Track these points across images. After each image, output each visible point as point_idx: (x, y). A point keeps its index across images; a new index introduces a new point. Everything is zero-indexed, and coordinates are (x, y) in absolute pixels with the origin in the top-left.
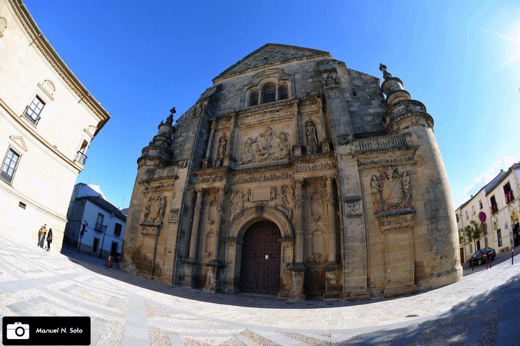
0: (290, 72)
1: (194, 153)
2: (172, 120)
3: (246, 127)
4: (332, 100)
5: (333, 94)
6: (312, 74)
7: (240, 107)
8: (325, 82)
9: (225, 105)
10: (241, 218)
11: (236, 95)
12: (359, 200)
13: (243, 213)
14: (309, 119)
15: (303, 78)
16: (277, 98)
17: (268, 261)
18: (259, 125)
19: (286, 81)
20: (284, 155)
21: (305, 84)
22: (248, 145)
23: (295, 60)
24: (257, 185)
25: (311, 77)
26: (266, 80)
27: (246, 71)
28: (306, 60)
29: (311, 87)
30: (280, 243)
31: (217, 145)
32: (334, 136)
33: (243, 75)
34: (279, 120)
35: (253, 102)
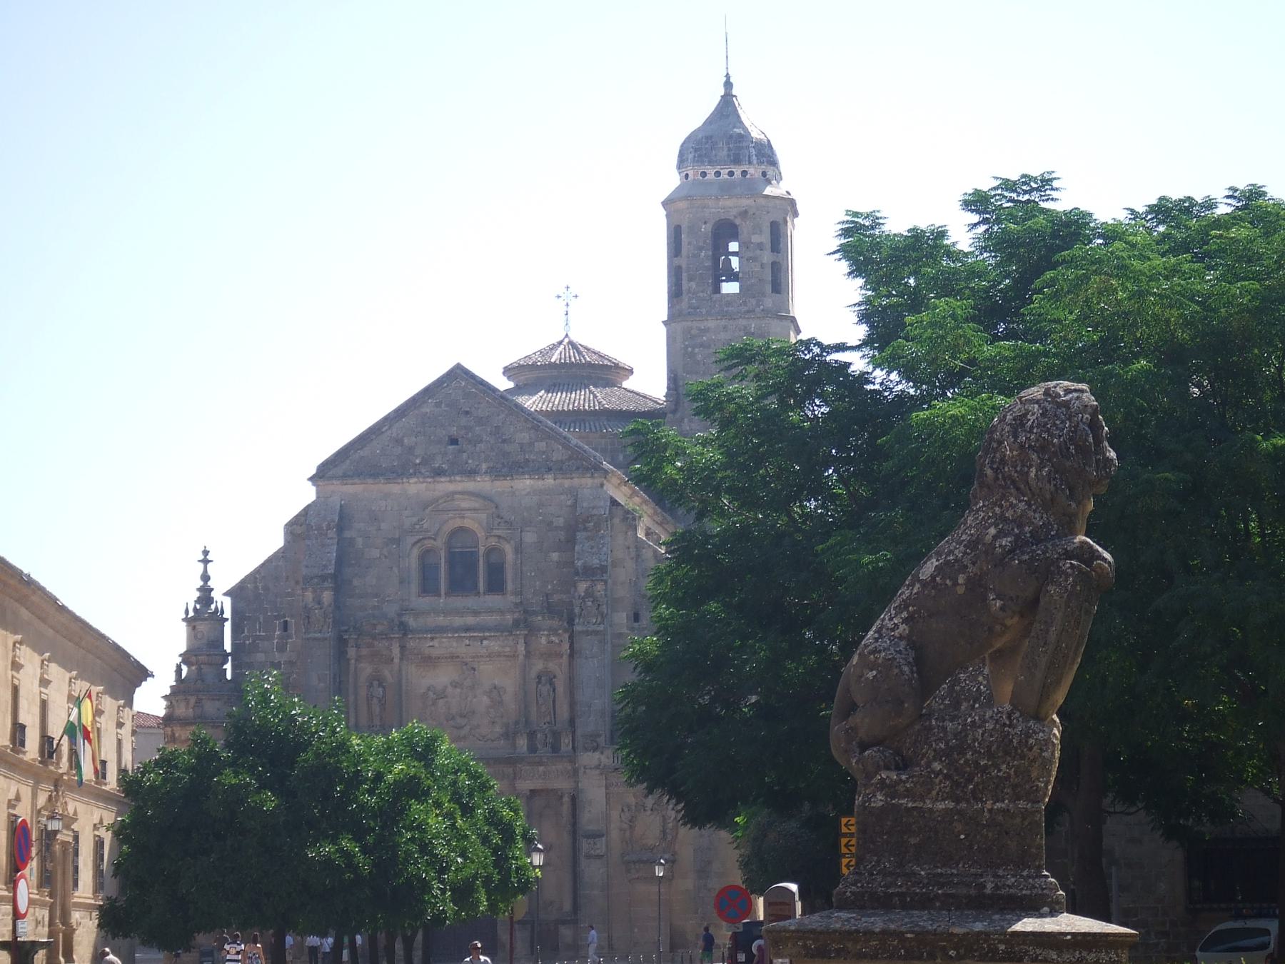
0: (513, 518)
2: (213, 589)
7: (403, 601)
11: (386, 557)
12: (603, 835)
16: (482, 586)
18: (449, 660)
19: (501, 540)
22: (431, 703)
23: (527, 477)
26: (458, 523)
27: (405, 480)
28: (551, 481)
31: (363, 692)
32: (579, 732)
33: (395, 488)
34: (489, 656)
35: (428, 586)
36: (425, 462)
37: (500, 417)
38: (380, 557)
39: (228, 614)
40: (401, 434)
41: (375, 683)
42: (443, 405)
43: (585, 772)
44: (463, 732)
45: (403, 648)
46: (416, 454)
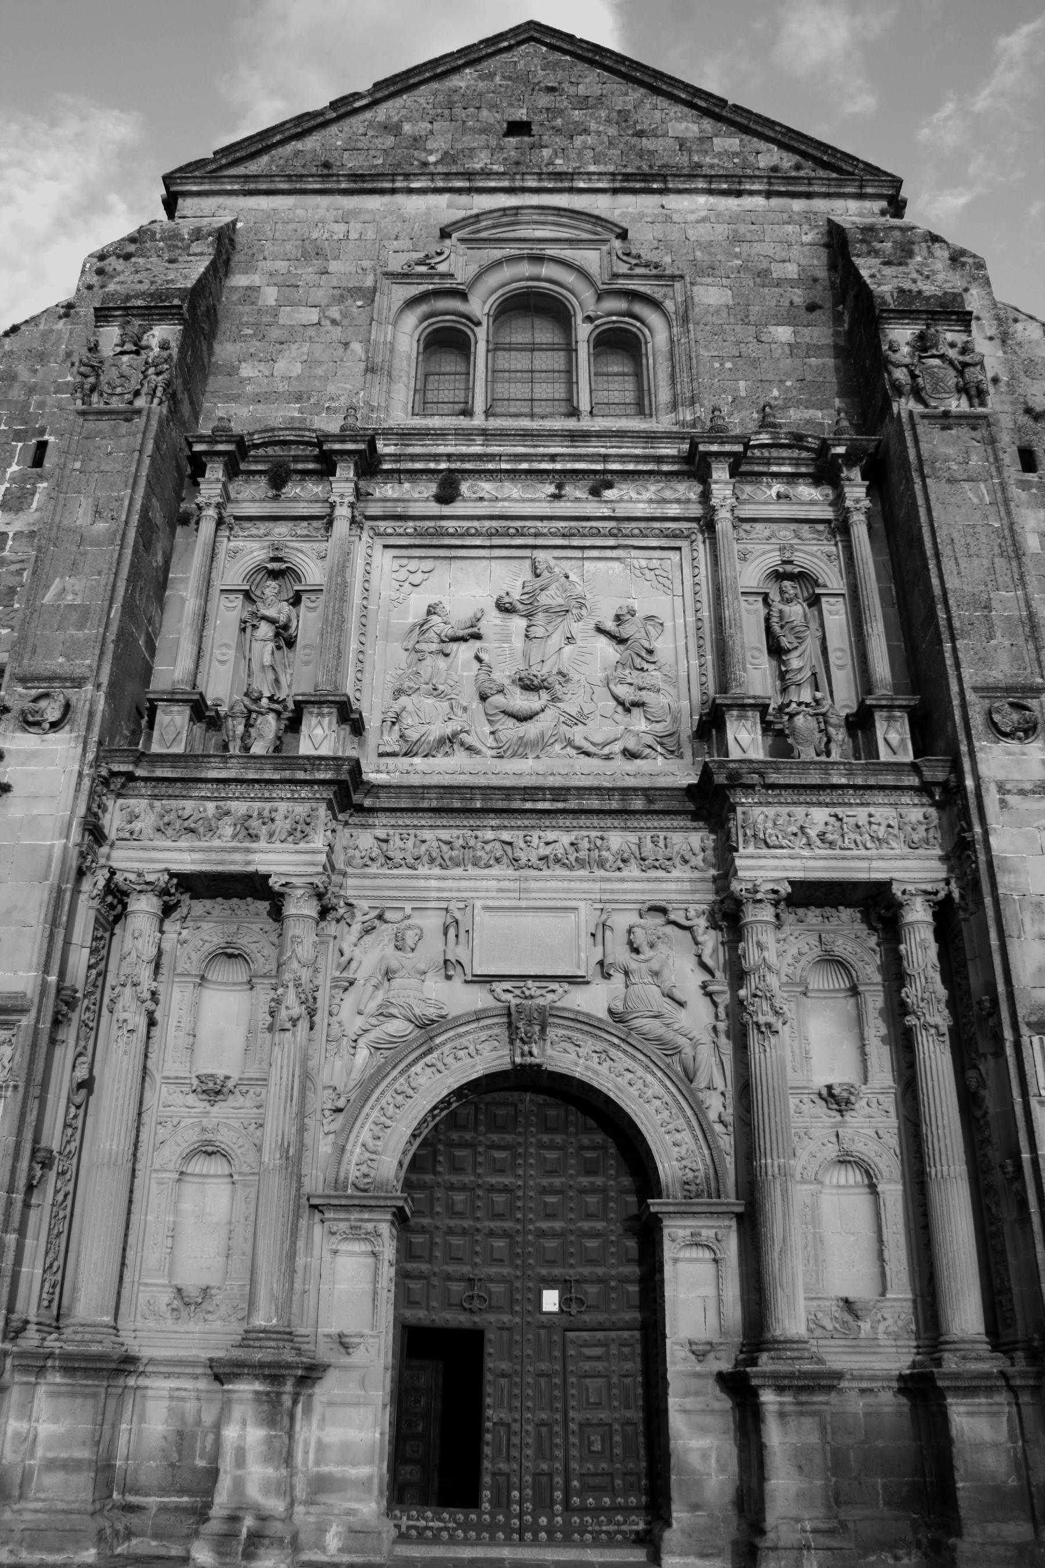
0: (668, 259)
1: (116, 642)
3: (418, 542)
4: (946, 487)
5: (951, 451)
6: (797, 300)
8: (904, 370)
9: (262, 367)
10: (418, 1068)
11: (334, 322)
13: (431, 1038)
14: (785, 562)
17: (548, 1324)
19: (639, 308)
20: (649, 740)
21: (752, 349)
22: (434, 647)
24: (505, 884)
25: (790, 320)
28: (760, 201)
29: (789, 376)
33: (374, 202)
37: (628, 98)
38: (319, 323)
40: (396, 119)
42: (498, 79)
43: (1002, 802)
44: (531, 730)
45: (358, 494)
46: (429, 147)
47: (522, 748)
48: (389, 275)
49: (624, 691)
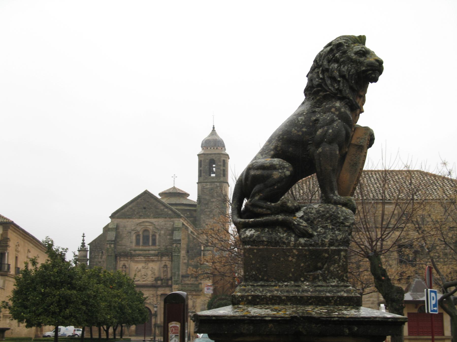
15: (165, 234)
16: (150, 244)
30: (151, 317)
32: (173, 280)
33: (131, 220)
35: (138, 243)
36: (137, 213)
39: (89, 249)
41: (124, 267)
47: (144, 281)
48: (132, 230)
49: (152, 276)
